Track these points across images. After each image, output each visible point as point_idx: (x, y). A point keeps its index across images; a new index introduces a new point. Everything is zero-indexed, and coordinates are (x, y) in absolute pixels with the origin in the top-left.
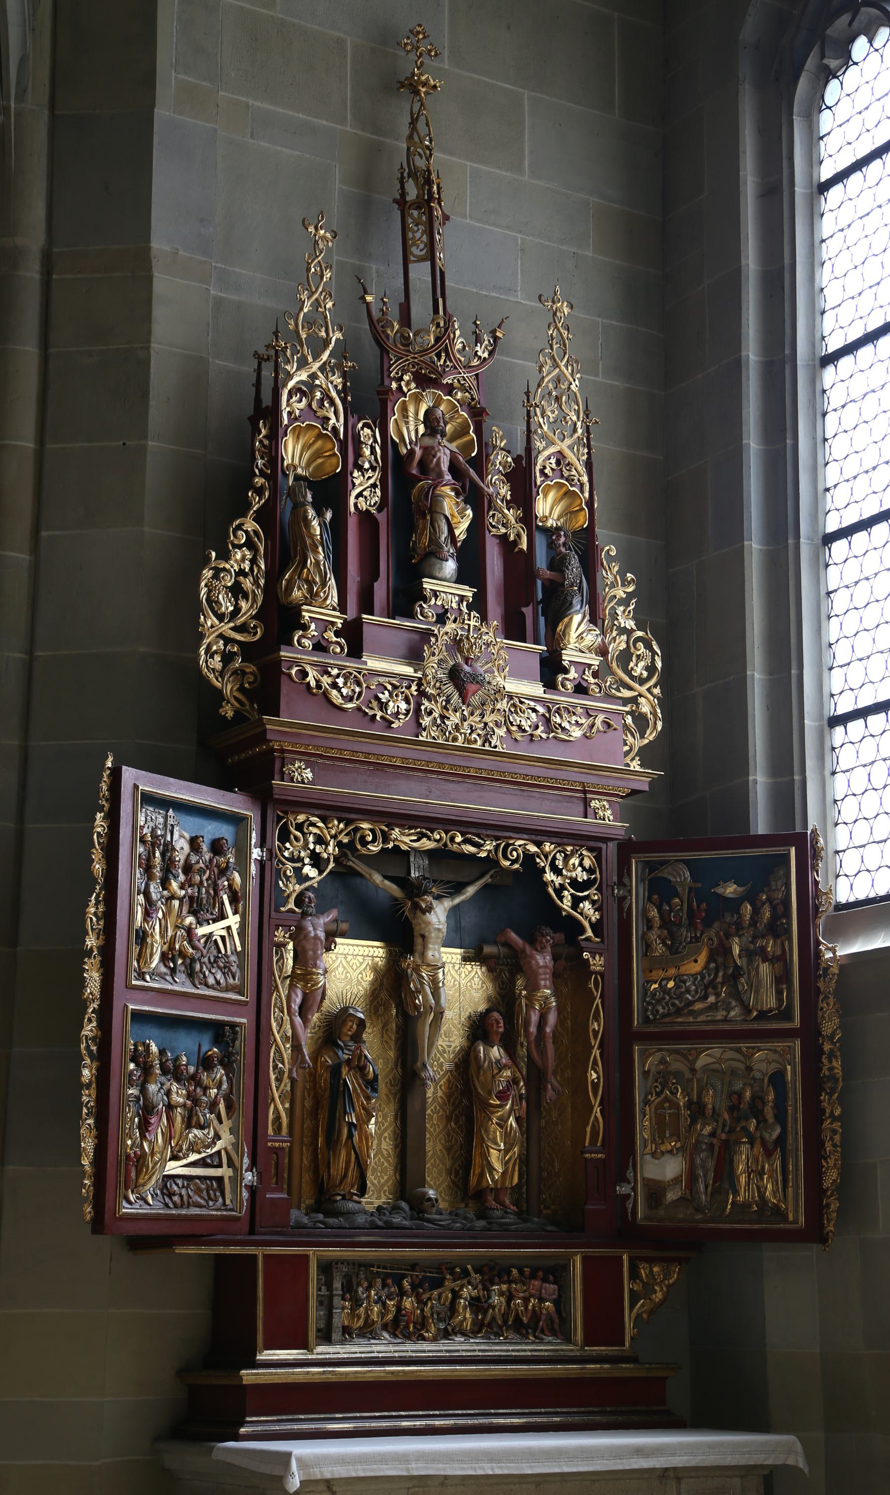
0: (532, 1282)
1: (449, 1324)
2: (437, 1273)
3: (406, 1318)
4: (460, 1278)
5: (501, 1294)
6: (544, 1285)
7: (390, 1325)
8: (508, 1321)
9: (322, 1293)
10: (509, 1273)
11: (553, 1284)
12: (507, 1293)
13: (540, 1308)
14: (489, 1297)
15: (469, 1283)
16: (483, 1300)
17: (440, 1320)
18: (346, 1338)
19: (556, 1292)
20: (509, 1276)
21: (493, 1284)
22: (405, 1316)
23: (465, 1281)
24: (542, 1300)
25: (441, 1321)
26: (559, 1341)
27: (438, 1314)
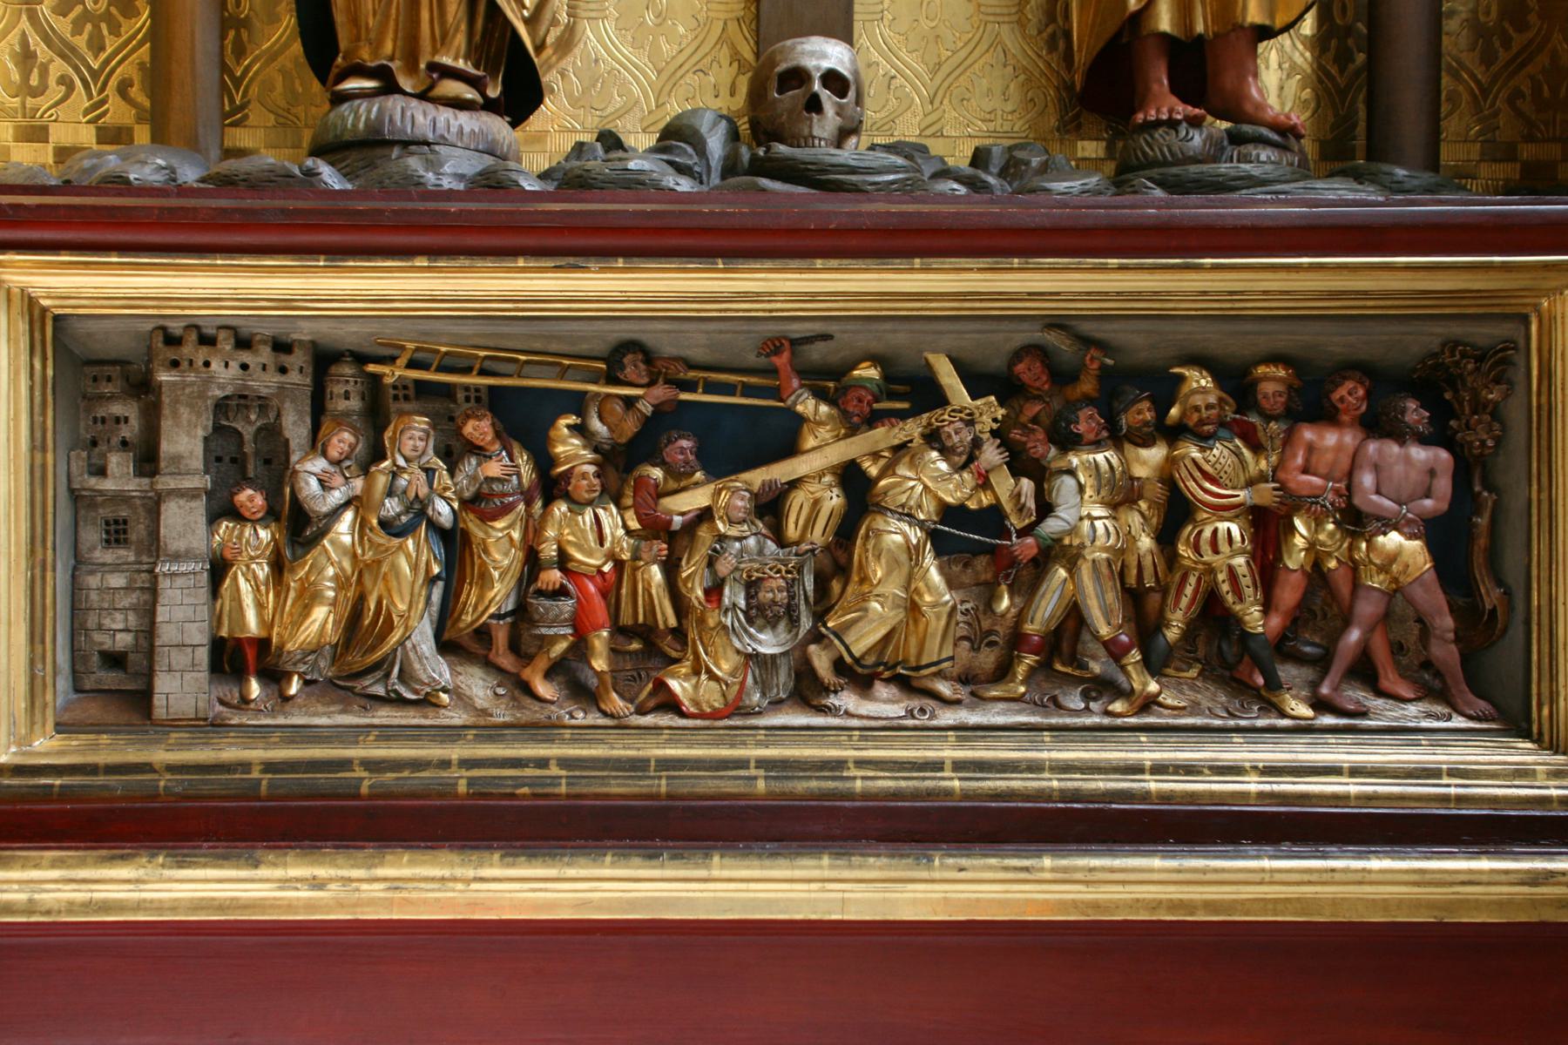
0: (1308, 434)
1: (816, 637)
2: (748, 391)
3: (567, 606)
4: (873, 419)
5: (1121, 495)
6: (1372, 447)
7: (501, 637)
8: (1161, 623)
9: (108, 485)
10: (1165, 389)
11: (1424, 441)
12: (1157, 491)
13: (1354, 568)
14: (1045, 508)
15: (933, 438)
16: (1016, 522)
17: (759, 614)
18: (245, 700)
19: (1444, 485)
20: (1162, 409)
21: (1068, 442)
22: (562, 592)
23: (913, 429)
24: (1356, 521)
25: (772, 623)
26: (1459, 722)
27: (752, 587)
